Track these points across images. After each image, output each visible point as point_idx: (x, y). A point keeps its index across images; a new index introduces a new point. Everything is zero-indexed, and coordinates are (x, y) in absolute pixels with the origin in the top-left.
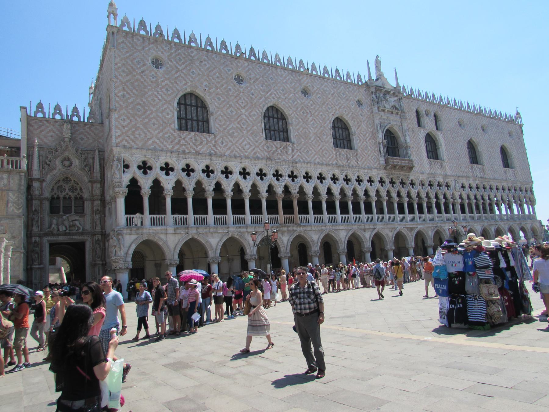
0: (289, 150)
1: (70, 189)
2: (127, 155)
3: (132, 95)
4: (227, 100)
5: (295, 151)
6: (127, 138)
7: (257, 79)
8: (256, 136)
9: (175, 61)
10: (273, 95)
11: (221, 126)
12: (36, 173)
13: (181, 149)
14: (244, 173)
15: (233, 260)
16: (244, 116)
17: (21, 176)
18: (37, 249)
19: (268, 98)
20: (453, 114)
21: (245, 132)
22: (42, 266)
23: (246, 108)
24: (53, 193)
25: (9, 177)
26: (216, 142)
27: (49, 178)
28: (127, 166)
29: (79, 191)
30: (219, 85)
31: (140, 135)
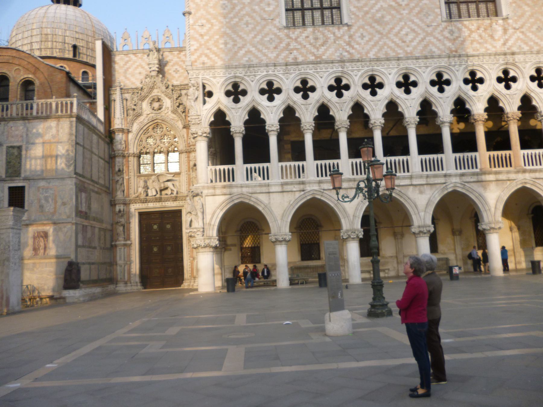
2: (208, 77)
5: (511, 31)
8: (427, 15)
11: (359, 9)
12: (117, 123)
13: (292, 56)
14: (406, 84)
15: (402, 235)
17: (71, 122)
18: (122, 220)
21: (405, 12)
22: (129, 242)
24: (141, 147)
25: (58, 125)
26: (351, 37)
27: (135, 127)
28: (210, 94)
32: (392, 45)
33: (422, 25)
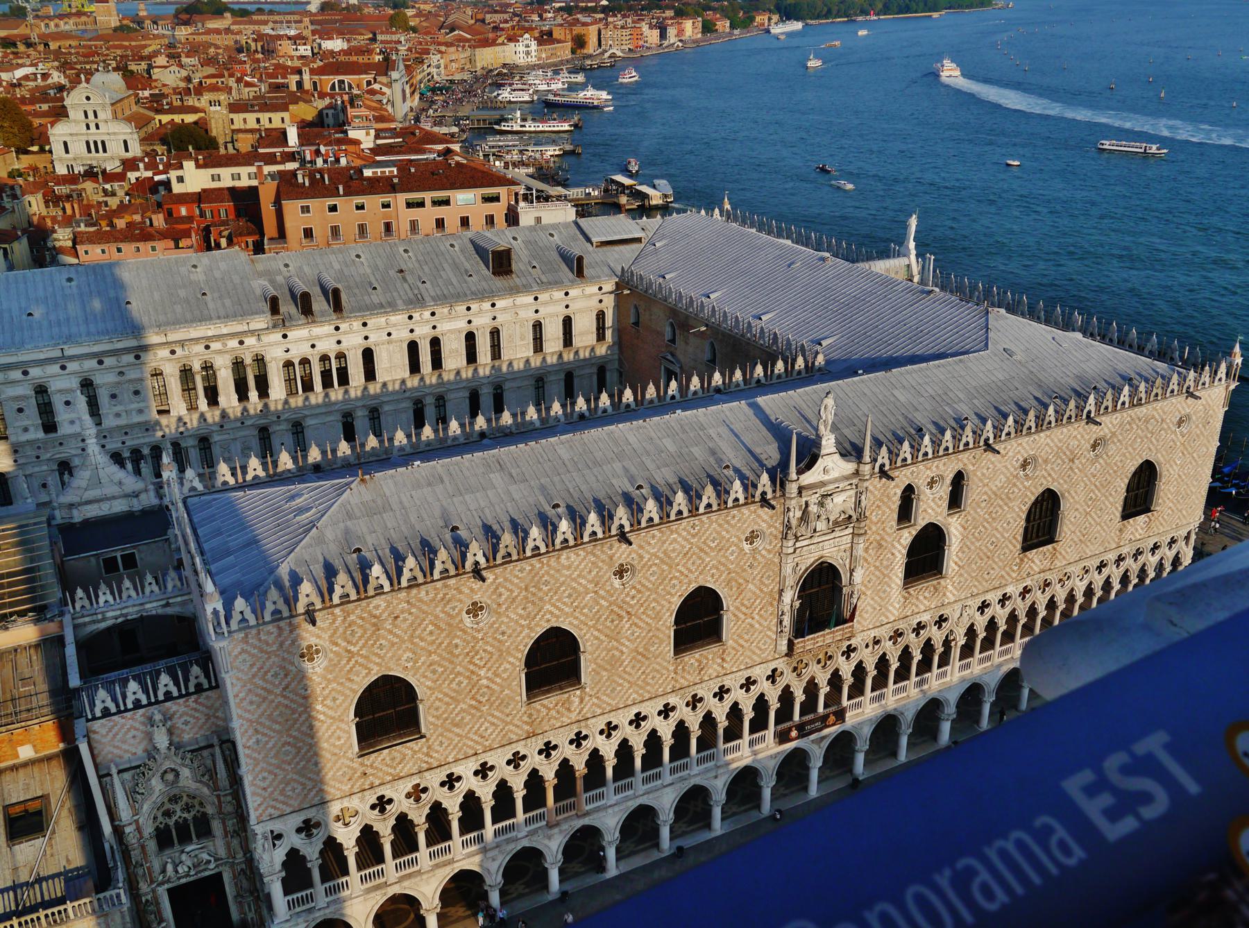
0: (571, 703)
1: (182, 810)
3: (272, 734)
4: (451, 666)
5: (587, 698)
6: (272, 803)
7: (514, 600)
9: (345, 640)
10: (548, 616)
16: (484, 682)
19: (537, 625)
20: (1010, 454)
23: (489, 665)
26: (429, 747)
29: (197, 807)
30: (432, 648)
31: (294, 790)
32: (470, 743)
33: (503, 717)
